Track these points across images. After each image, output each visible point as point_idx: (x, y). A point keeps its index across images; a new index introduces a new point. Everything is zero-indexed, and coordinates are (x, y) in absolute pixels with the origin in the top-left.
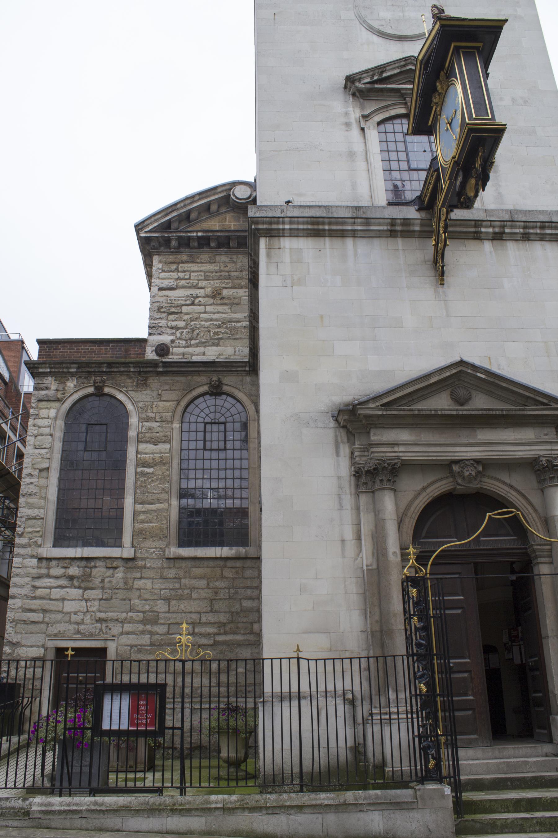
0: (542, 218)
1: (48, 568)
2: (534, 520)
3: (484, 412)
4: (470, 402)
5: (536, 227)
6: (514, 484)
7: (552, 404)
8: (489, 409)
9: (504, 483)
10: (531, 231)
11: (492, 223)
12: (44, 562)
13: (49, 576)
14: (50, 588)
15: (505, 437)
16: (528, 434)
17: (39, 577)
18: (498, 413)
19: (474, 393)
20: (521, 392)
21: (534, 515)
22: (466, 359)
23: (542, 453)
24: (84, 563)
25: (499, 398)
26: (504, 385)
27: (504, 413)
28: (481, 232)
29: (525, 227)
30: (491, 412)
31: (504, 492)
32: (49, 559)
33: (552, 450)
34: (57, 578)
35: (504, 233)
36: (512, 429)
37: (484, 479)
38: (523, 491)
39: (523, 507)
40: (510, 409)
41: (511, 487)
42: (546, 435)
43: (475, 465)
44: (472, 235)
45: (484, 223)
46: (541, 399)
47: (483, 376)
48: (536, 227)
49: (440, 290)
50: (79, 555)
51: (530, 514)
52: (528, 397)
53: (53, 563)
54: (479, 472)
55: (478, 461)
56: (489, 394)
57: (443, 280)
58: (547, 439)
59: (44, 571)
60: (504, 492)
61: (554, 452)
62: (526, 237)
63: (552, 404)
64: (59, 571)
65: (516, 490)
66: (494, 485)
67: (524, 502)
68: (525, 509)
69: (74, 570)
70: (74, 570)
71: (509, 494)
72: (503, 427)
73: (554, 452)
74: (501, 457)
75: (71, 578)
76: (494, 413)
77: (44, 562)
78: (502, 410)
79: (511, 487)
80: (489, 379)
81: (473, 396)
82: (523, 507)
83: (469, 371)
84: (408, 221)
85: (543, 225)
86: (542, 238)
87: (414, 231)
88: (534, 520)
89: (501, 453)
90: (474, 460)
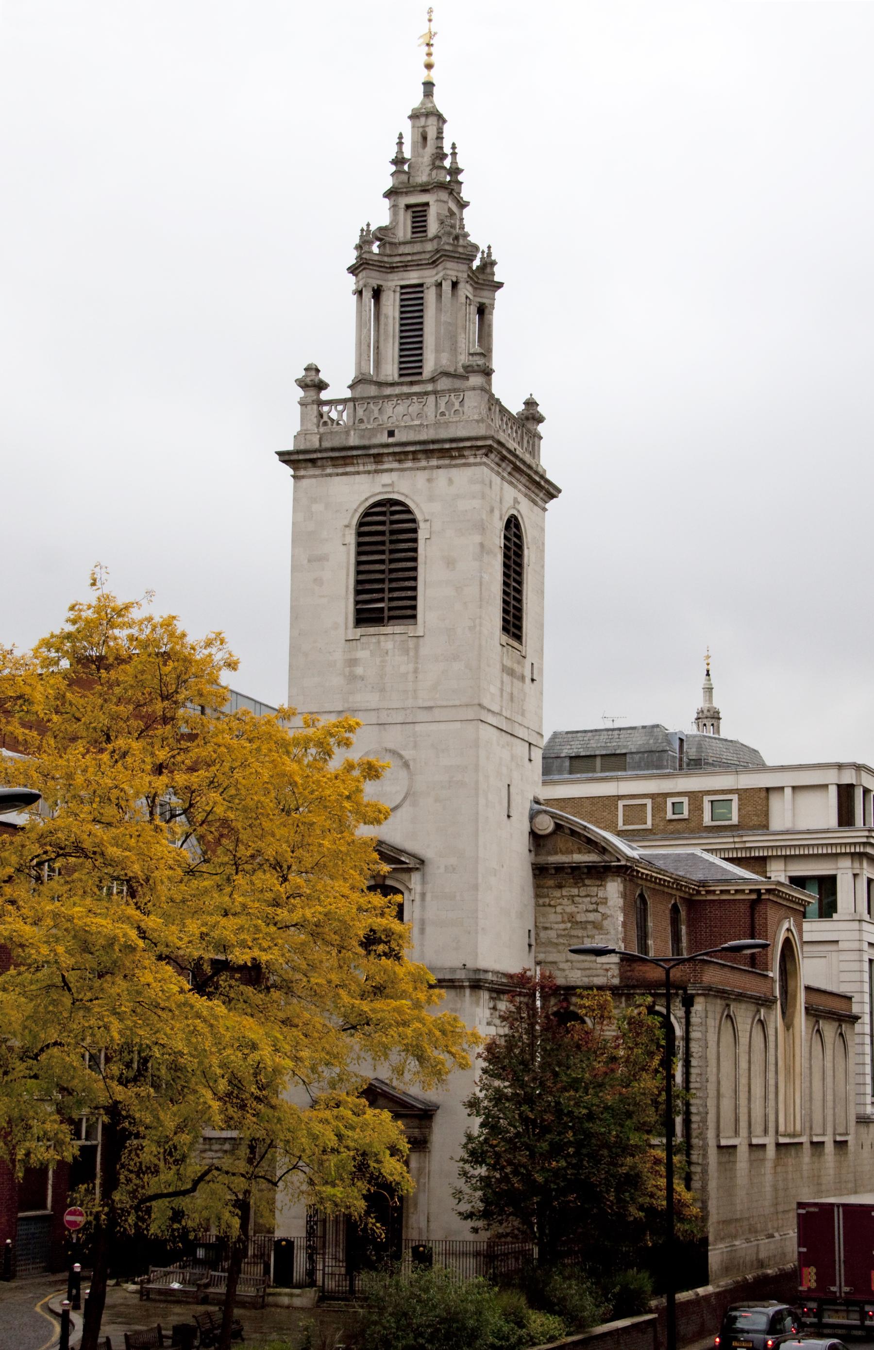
1: (211, 1145)
12: (207, 1142)
13: (211, 1150)
14: (213, 1158)
17: (204, 1151)
24: (233, 1142)
32: (210, 1139)
34: (216, 1151)
50: (229, 1136)
53: (214, 1141)
59: (207, 1147)
64: (216, 1147)
69: (227, 1147)
70: (227, 1147)
75: (226, 1152)
77: (207, 1142)
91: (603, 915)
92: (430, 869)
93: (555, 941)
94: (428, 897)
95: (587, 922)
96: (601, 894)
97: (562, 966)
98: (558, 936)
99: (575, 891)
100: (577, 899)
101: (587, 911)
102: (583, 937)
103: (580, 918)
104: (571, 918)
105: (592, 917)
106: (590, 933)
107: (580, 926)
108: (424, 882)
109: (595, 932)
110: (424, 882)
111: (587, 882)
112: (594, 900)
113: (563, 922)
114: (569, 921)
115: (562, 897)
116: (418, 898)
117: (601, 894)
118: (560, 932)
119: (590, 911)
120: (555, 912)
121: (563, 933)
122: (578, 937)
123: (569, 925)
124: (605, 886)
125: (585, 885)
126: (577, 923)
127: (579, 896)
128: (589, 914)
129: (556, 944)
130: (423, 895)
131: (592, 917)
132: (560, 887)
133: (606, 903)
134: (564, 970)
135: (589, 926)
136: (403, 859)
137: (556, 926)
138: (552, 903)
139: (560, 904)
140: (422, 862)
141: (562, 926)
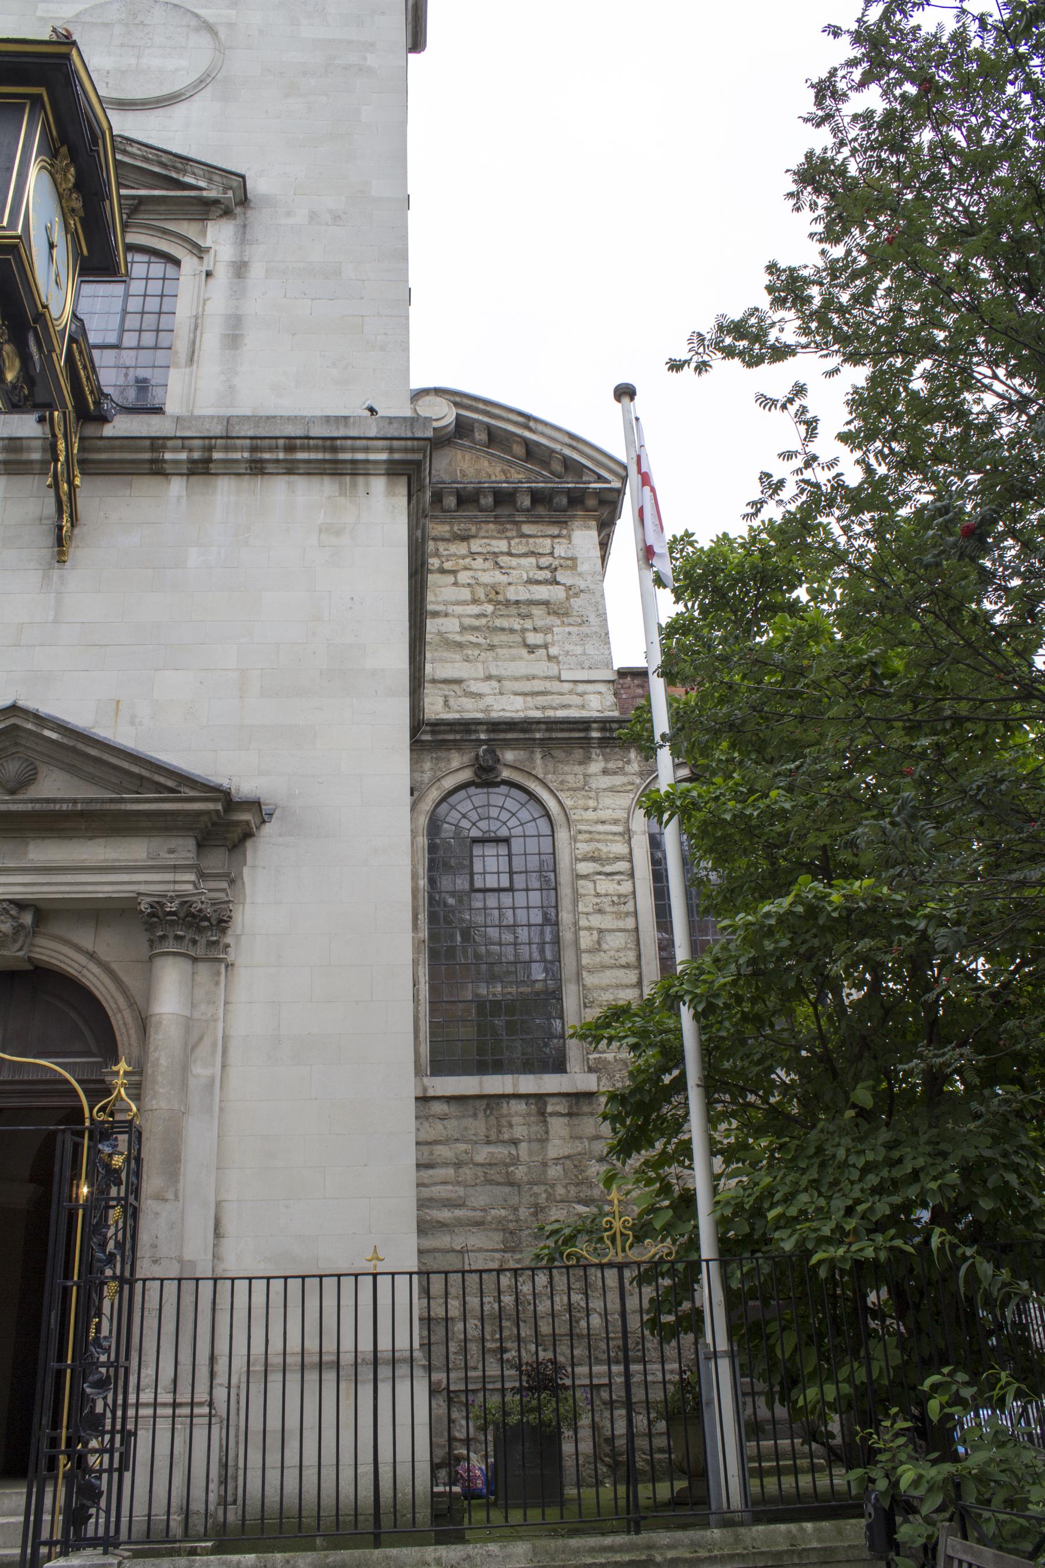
0: (290, 430)
2: (125, 1024)
3: (38, 807)
4: (33, 787)
5: (277, 447)
6: (103, 954)
7: (187, 790)
8: (48, 801)
9: (78, 948)
10: (267, 456)
11: (186, 442)
15: (85, 857)
16: (134, 850)
18: (64, 807)
19: (43, 770)
20: (126, 765)
21: (127, 1014)
22: (21, 703)
23: (142, 888)
25: (92, 779)
26: (93, 752)
27: (79, 807)
28: (164, 461)
29: (254, 449)
30: (51, 806)
31: (76, 966)
33: (175, 882)
35: (210, 460)
36: (102, 841)
37: (41, 941)
38: (114, 966)
39: (108, 997)
40: (92, 801)
41: (92, 956)
42: (171, 851)
43: (13, 912)
44: (147, 466)
45: (169, 443)
46: (162, 780)
47: (54, 736)
48: (277, 447)
49: (56, 573)
51: (120, 1011)
52: (142, 778)
54: (22, 926)
55: (21, 905)
56: (72, 770)
57: (61, 553)
58: (171, 859)
60: (76, 966)
61: (178, 887)
62: (257, 468)
63: (182, 789)
65: (99, 963)
66: (55, 952)
67: (112, 986)
68: (111, 1001)
71: (85, 972)
72: (84, 837)
73: (178, 887)
74: (66, 896)
76: (57, 807)
78: (75, 801)
79: (92, 956)
80: (65, 741)
81: (40, 777)
82: (108, 997)
83: (30, 726)
84: (18, 442)
85: (291, 444)
86: (291, 469)
87: (31, 462)
88: (125, 1024)
89: (68, 888)
90: (11, 901)
91: (569, 588)
92: (259, 218)
93: (458, 638)
94: (256, 270)
95: (531, 603)
96: (560, 551)
97: (475, 687)
98: (464, 629)
99: (502, 545)
100: (506, 558)
101: (530, 582)
102: (524, 630)
103: (512, 594)
104: (495, 595)
105: (542, 592)
106: (539, 623)
107: (513, 610)
108: (243, 237)
109: (552, 620)
110: (243, 237)
111: (527, 529)
112: (544, 561)
113: (475, 601)
114: (490, 601)
115: (473, 555)
116: (223, 274)
117: (560, 551)
118: (467, 621)
119: (538, 582)
120: (456, 584)
121: (476, 623)
122: (512, 631)
123: (489, 608)
124: (569, 537)
125: (523, 536)
126: (508, 603)
127: (510, 554)
128: (535, 588)
129: (460, 645)
130: (240, 269)
131: (542, 592)
132: (465, 538)
133: (574, 568)
134: (480, 695)
135: (537, 611)
136: (189, 179)
137: (459, 609)
138: (447, 565)
139: (466, 569)
140: (244, 201)
141: (475, 609)
